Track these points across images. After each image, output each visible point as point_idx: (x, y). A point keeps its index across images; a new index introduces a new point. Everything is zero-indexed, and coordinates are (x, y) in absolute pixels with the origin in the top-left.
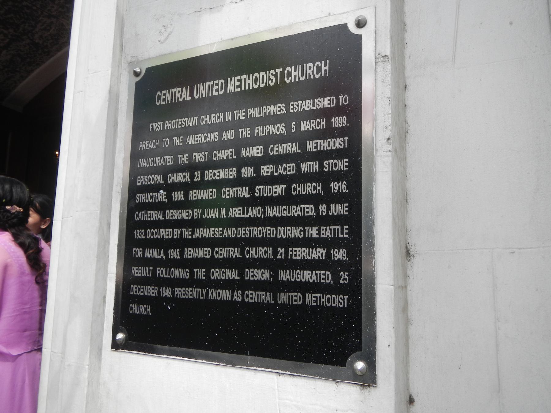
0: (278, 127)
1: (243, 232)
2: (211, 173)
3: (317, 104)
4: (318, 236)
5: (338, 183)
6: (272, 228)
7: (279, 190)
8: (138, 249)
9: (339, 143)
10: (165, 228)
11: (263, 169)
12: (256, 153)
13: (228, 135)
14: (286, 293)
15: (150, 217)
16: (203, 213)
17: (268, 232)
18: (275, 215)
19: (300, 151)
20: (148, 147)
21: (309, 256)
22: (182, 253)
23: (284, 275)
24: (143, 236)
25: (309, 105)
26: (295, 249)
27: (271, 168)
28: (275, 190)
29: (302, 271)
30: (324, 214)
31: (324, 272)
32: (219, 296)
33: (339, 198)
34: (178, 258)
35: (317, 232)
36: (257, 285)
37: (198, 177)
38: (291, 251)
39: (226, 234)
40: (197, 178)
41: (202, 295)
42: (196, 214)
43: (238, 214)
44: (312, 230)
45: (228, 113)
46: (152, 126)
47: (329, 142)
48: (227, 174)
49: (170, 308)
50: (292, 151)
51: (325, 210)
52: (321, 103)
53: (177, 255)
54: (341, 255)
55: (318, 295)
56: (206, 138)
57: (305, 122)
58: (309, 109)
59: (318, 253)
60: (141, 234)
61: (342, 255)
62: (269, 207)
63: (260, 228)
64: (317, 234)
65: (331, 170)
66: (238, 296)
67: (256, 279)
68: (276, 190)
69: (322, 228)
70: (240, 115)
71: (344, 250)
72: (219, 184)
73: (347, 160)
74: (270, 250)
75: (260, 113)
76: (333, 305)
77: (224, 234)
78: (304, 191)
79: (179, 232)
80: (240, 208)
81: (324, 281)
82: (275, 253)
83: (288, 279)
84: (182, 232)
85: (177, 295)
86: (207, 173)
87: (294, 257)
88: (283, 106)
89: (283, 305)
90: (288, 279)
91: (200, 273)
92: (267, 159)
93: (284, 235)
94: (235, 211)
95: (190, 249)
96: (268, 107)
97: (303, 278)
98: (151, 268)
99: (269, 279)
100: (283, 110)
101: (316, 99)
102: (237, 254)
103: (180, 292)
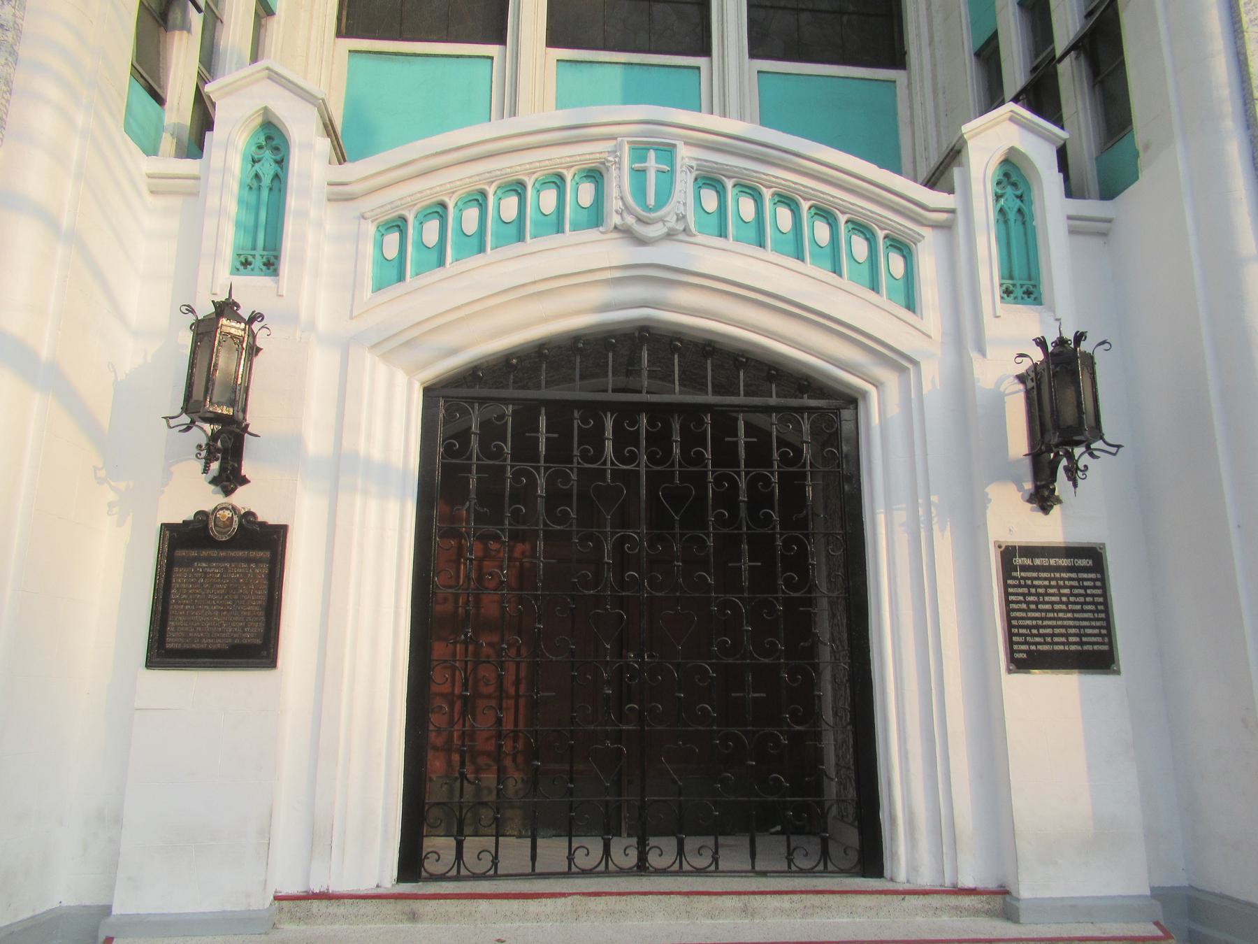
1: (1066, 623)
7: (1079, 607)
9: (1099, 592)
13: (1053, 583)
17: (1077, 623)
22: (1038, 631)
23: (1084, 639)
33: (1101, 612)
36: (1074, 643)
59: (1096, 631)
70: (1058, 575)
72: (1052, 603)
89: (1086, 651)
91: (1049, 639)
103: (1040, 647)
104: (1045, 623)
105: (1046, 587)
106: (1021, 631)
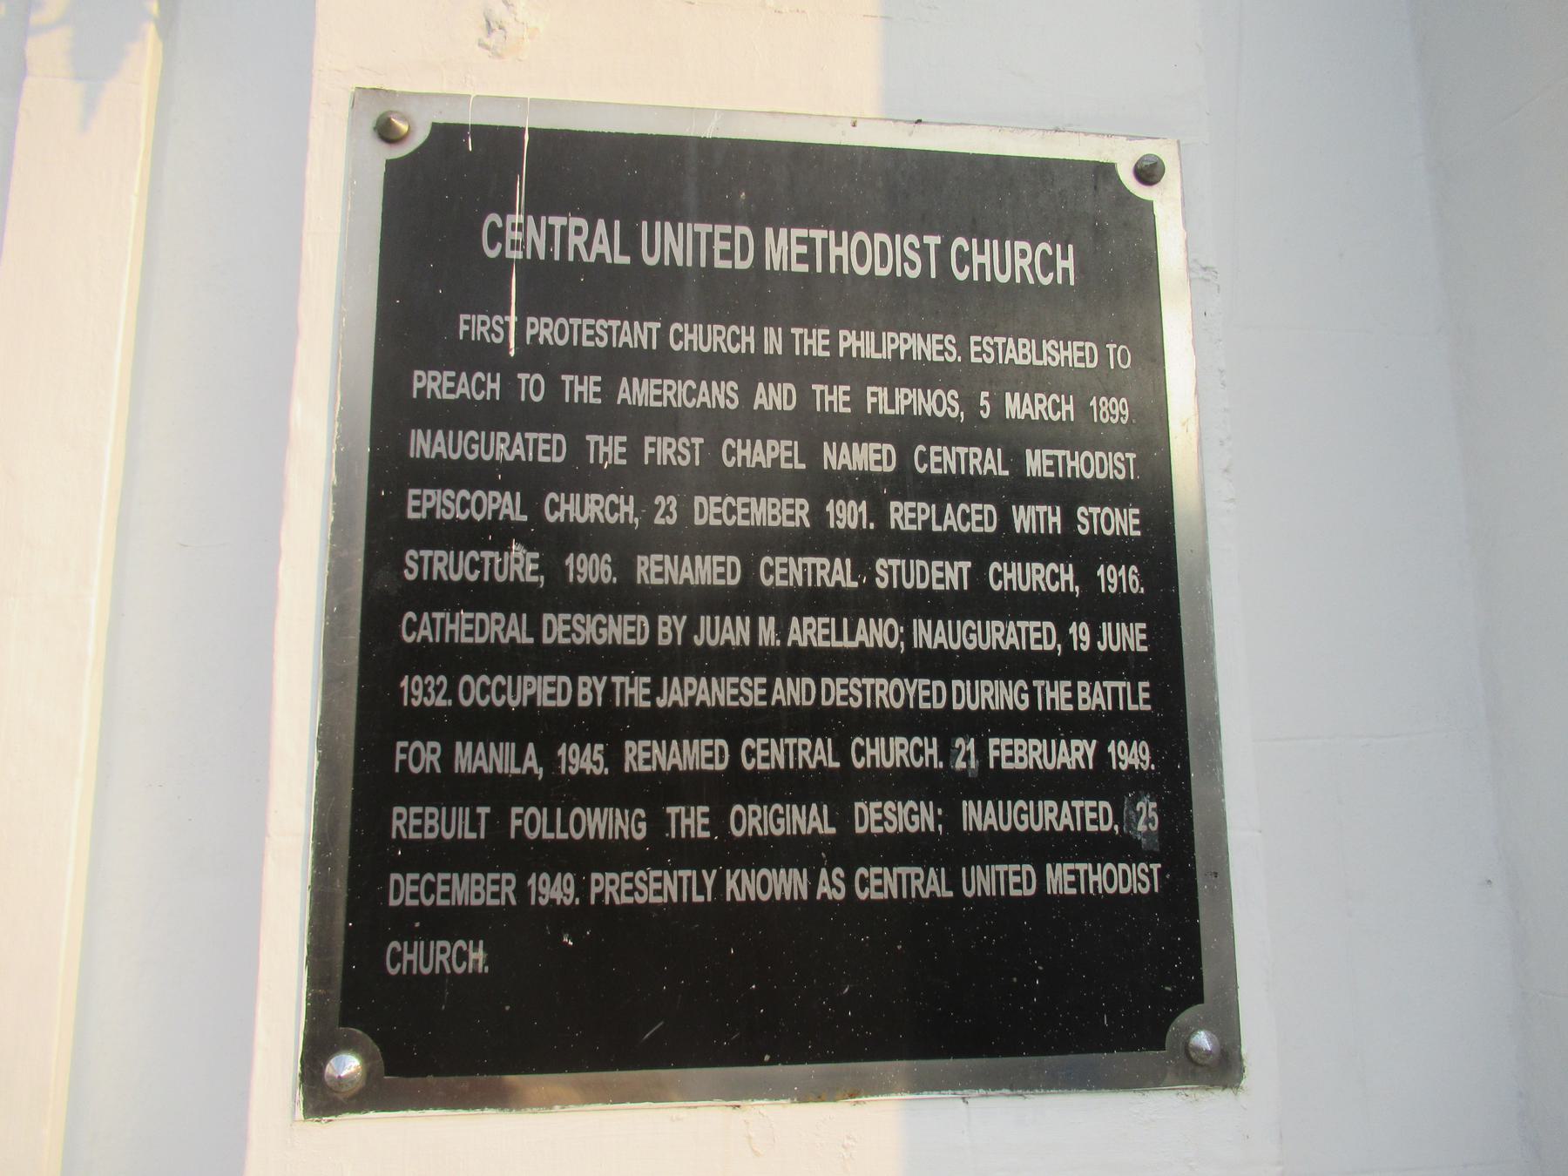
0: (939, 397)
1: (840, 691)
2: (719, 505)
3: (1049, 354)
4: (1070, 707)
5: (1118, 569)
6: (933, 682)
7: (952, 574)
8: (418, 744)
10: (538, 671)
11: (897, 510)
12: (1045, 469)
13: (775, 397)
14: (987, 867)
15: (470, 633)
16: (692, 628)
17: (924, 692)
18: (941, 645)
19: (1006, 473)
20: (451, 391)
21: (1050, 761)
22: (614, 757)
23: (977, 816)
24: (444, 698)
25: (1027, 351)
26: (1009, 741)
27: (923, 511)
28: (937, 574)
29: (1031, 803)
30: (1085, 648)
31: (1093, 804)
32: (765, 890)
33: (1121, 608)
34: (598, 772)
35: (1069, 695)
37: (667, 513)
38: (997, 747)
39: (782, 696)
40: (663, 516)
41: (702, 889)
42: (668, 630)
43: (820, 637)
44: (1052, 689)
45: (769, 332)
46: (468, 322)
47: (1087, 459)
48: (778, 514)
49: (571, 943)
50: (983, 469)
51: (1087, 638)
52: (1059, 353)
53: (597, 763)
54: (1136, 756)
55: (1081, 867)
56: (692, 394)
57: (1017, 395)
58: (1027, 362)
59: (1075, 753)
60: (431, 689)
61: (1139, 757)
62: (920, 621)
63: (896, 681)
64: (1068, 701)
65: (1096, 533)
66: (832, 885)
67: (891, 830)
68: (941, 575)
69: (1081, 684)
70: (815, 342)
71: (1143, 743)
73: (1137, 511)
74: (931, 746)
75: (878, 349)
76: (1124, 891)
77: (775, 697)
78: (1024, 582)
79: (600, 688)
80: (826, 620)
81: (1095, 828)
82: (946, 752)
83: (991, 827)
84: (610, 688)
85: (600, 896)
86: (701, 505)
87: (1005, 765)
88: (950, 342)
89: (981, 901)
90: (991, 827)
91: (692, 821)
92: (906, 483)
93: (973, 700)
94: (810, 626)
95: (647, 743)
96: (903, 335)
97: (1037, 822)
98: (483, 811)
99: (932, 829)
100: (951, 354)
101: (1044, 341)
102: (823, 757)
103: (610, 886)
104: (678, 693)
105: (714, 424)
106: (467, 758)
